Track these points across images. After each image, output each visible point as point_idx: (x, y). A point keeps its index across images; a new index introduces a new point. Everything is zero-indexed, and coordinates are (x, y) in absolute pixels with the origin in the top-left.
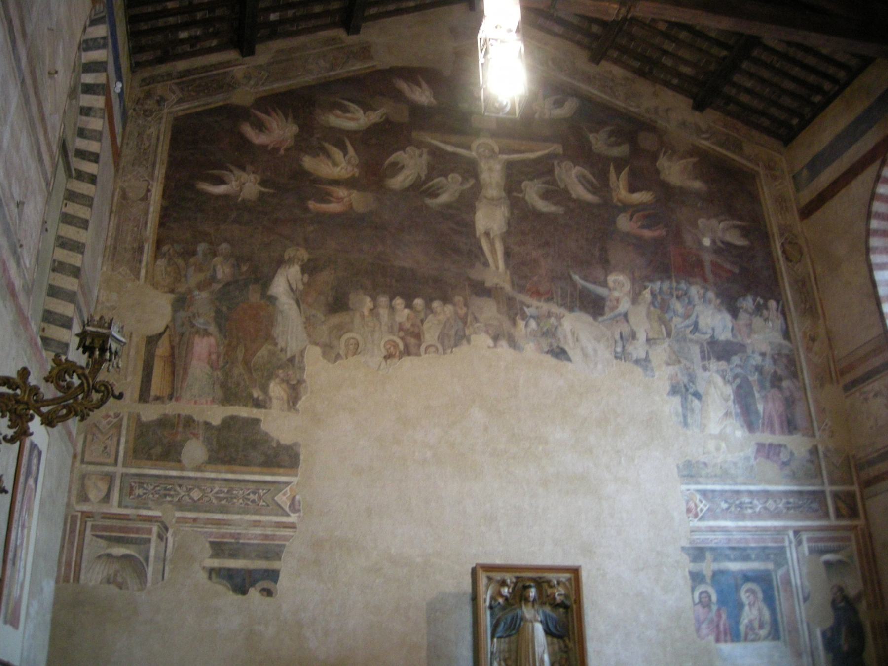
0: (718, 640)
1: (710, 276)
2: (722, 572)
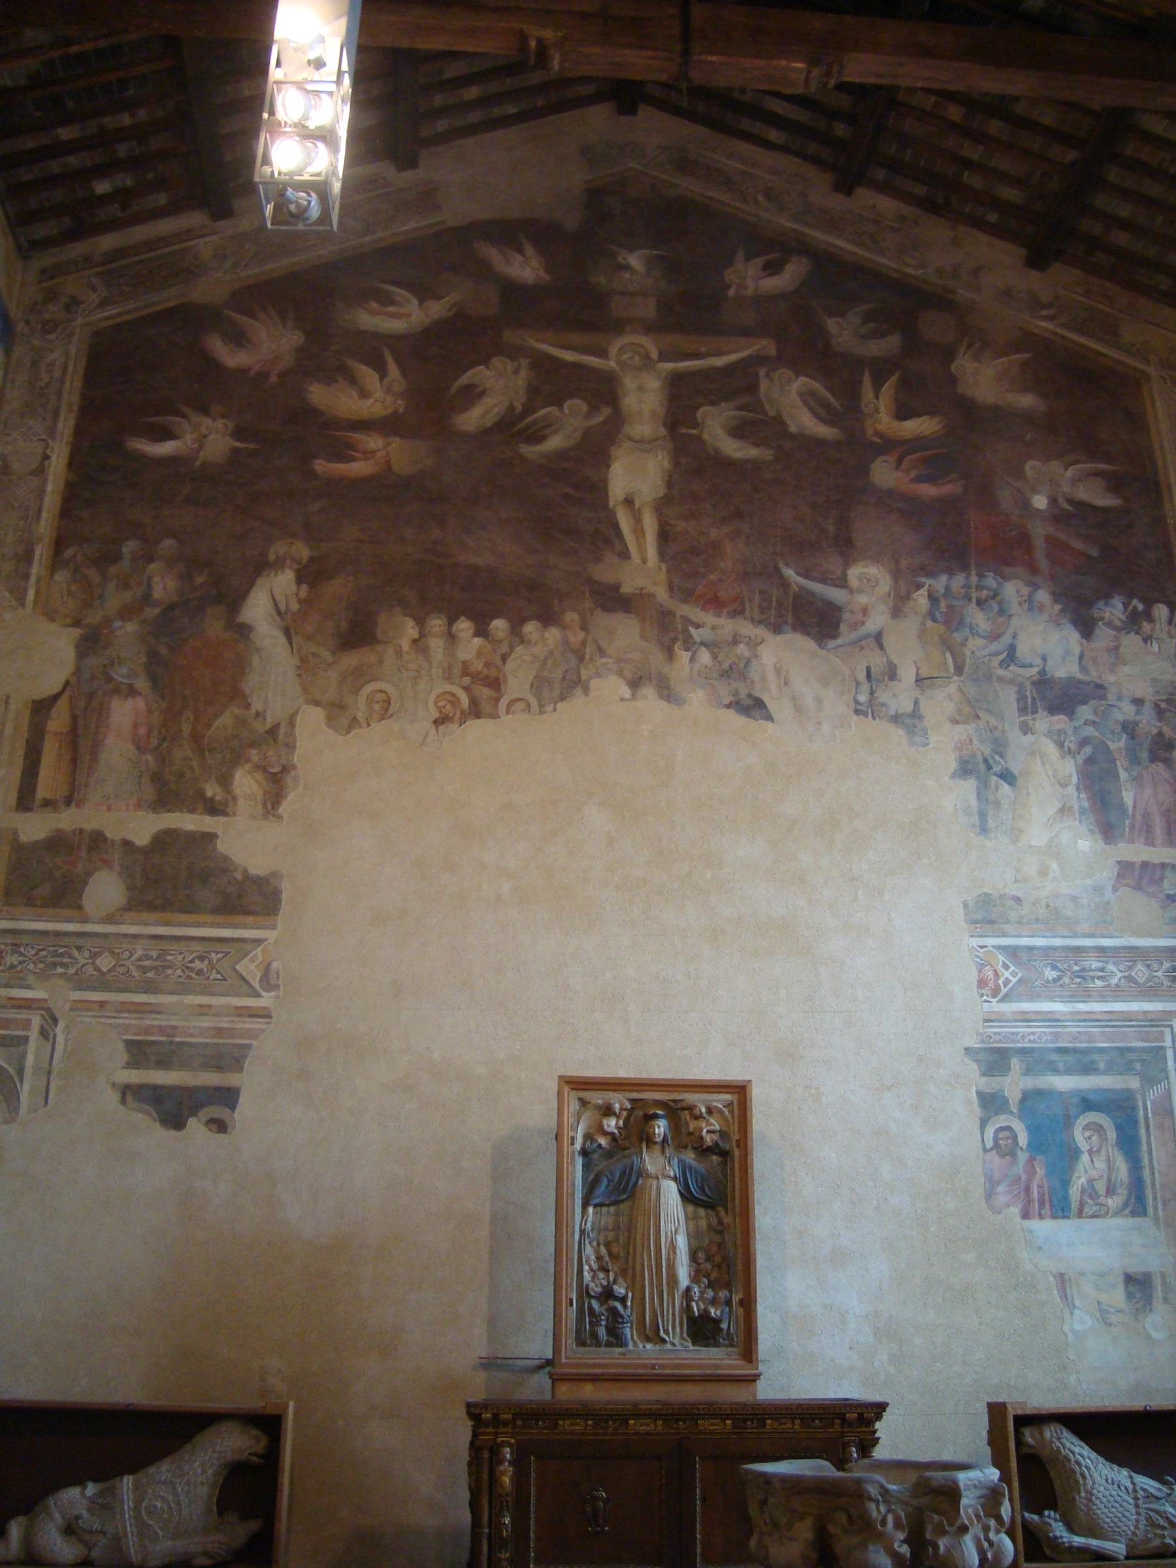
0: (1026, 1215)
1: (1043, 564)
2: (1040, 1093)
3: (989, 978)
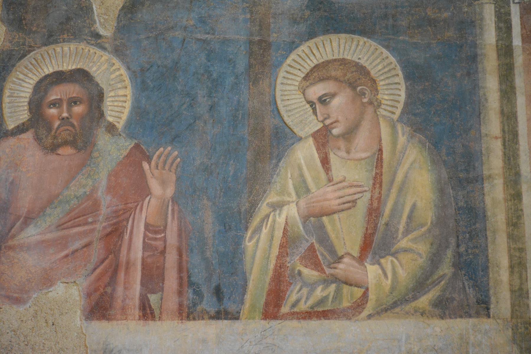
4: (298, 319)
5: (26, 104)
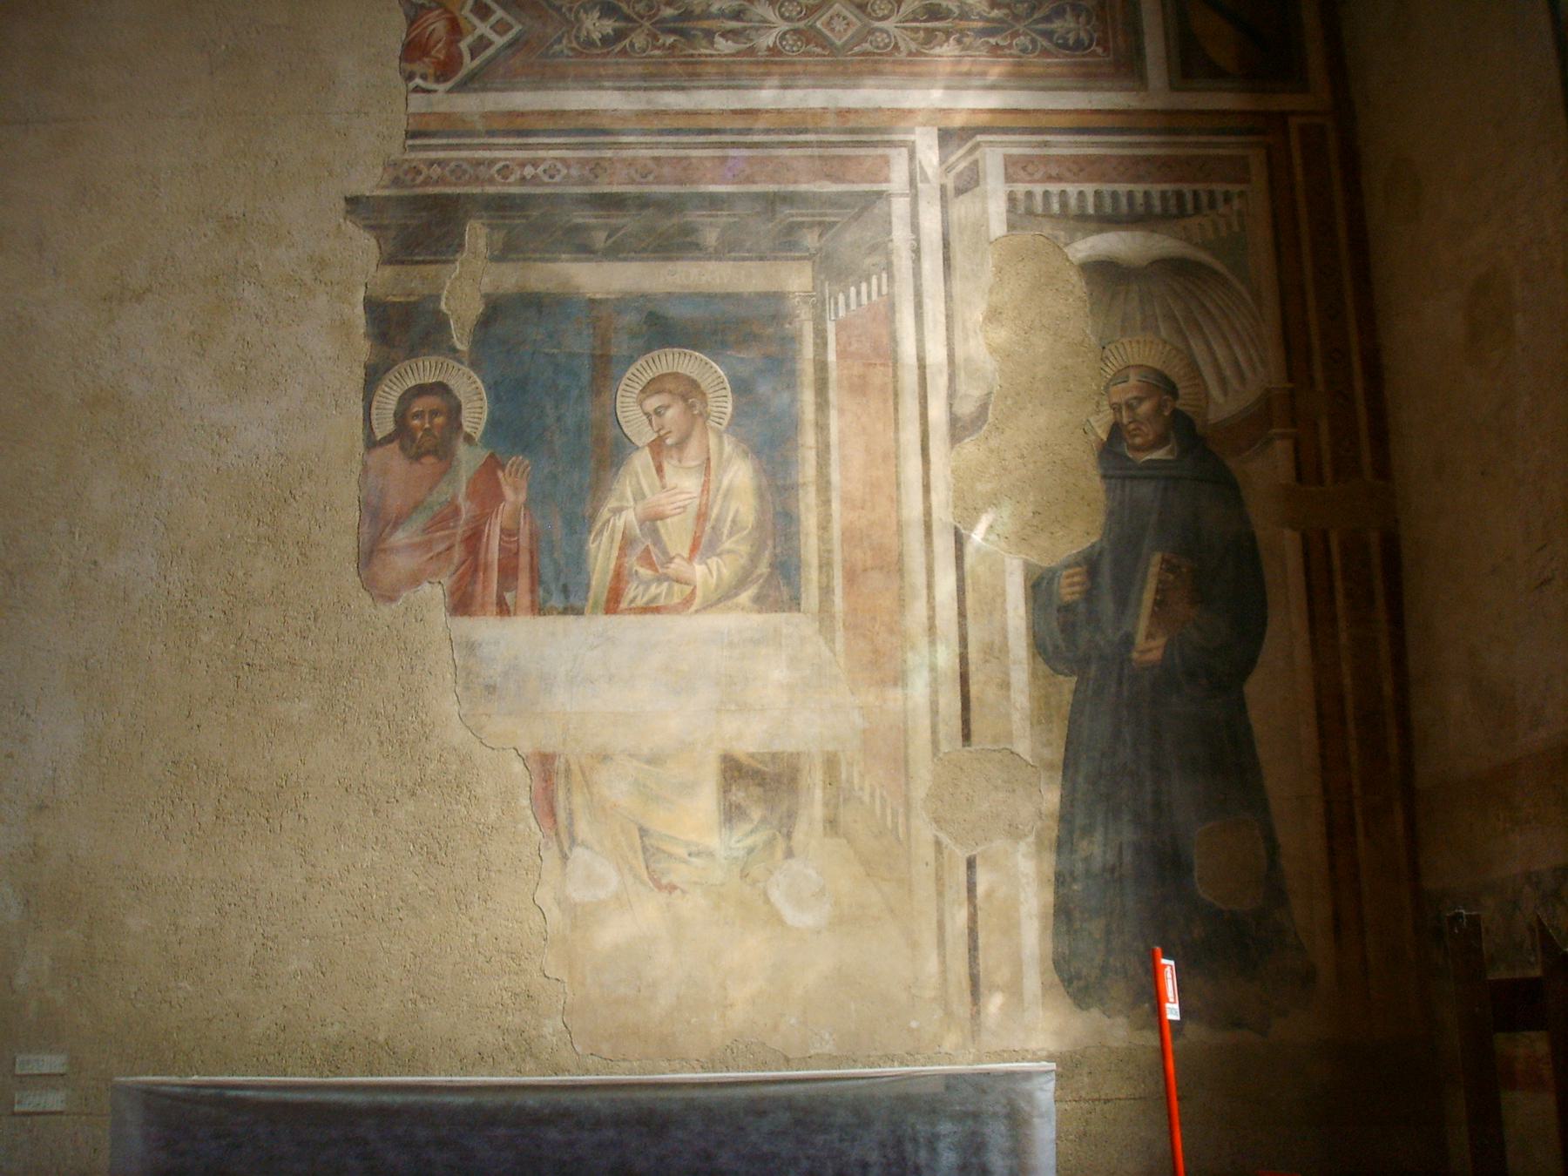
0: (462, 604)
2: (535, 304)
3: (435, 37)
4: (635, 613)
5: (392, 415)
